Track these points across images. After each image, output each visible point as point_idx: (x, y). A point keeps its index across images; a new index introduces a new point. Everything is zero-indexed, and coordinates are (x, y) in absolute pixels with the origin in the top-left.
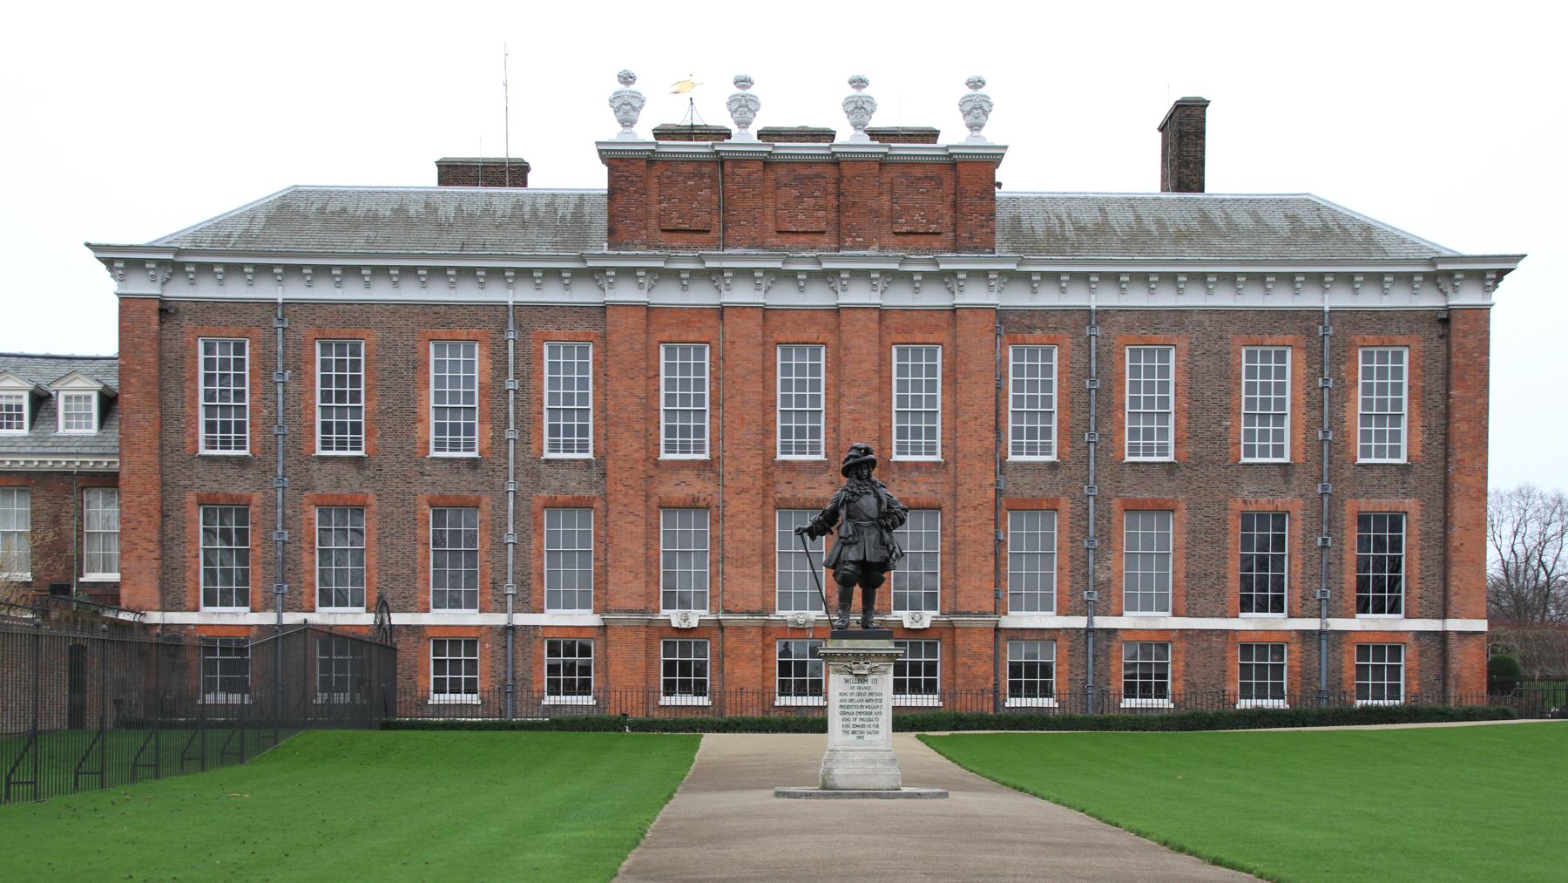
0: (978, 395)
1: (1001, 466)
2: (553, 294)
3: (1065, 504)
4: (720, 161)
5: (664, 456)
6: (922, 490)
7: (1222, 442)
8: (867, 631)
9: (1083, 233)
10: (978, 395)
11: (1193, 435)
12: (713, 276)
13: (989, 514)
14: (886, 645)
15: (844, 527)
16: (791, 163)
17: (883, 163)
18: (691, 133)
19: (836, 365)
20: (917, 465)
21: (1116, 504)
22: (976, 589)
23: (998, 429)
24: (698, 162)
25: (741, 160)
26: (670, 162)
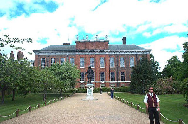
0: (108, 62)
1: (110, 68)
2: (71, 54)
3: (115, 71)
4: (85, 42)
5: (80, 68)
6: (103, 70)
7: (129, 65)
8: (91, 83)
9: (117, 49)
10: (108, 62)
11: (126, 65)
12: (85, 52)
13: (109, 72)
14: (92, 85)
15: (88, 74)
16: (91, 42)
17: (99, 42)
18: (84, 40)
19: (95, 59)
20: (102, 68)
21: (120, 71)
22: (108, 79)
23: (110, 65)
24: (83, 42)
25: (87, 42)
26: (81, 42)
